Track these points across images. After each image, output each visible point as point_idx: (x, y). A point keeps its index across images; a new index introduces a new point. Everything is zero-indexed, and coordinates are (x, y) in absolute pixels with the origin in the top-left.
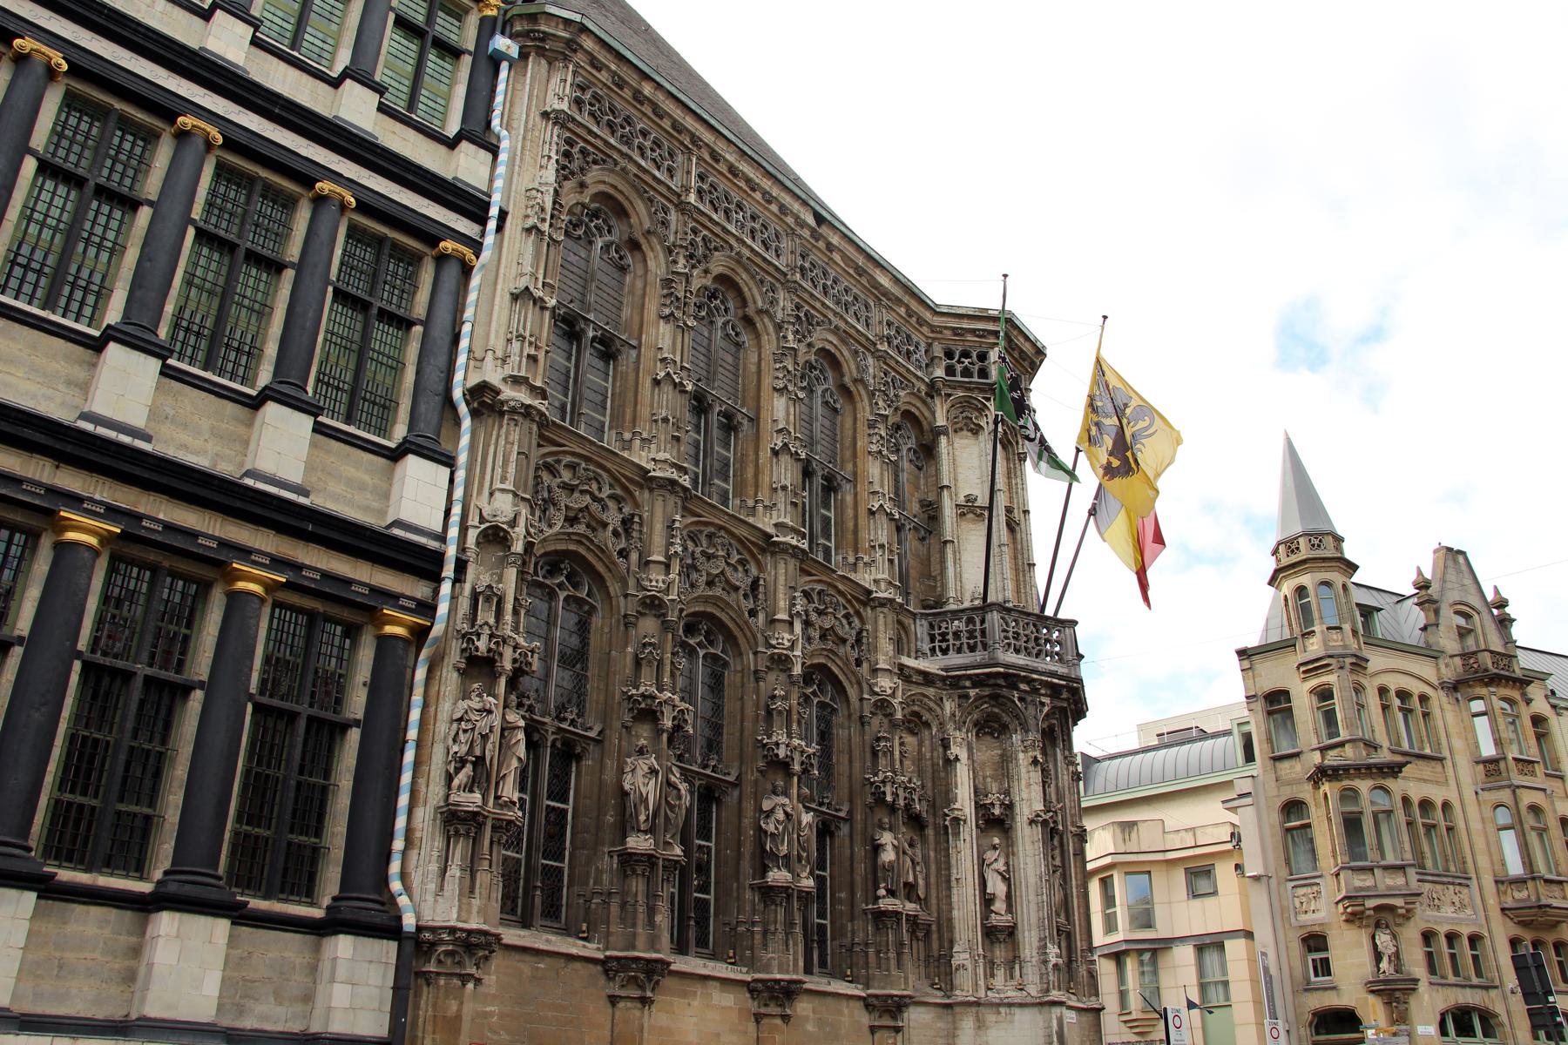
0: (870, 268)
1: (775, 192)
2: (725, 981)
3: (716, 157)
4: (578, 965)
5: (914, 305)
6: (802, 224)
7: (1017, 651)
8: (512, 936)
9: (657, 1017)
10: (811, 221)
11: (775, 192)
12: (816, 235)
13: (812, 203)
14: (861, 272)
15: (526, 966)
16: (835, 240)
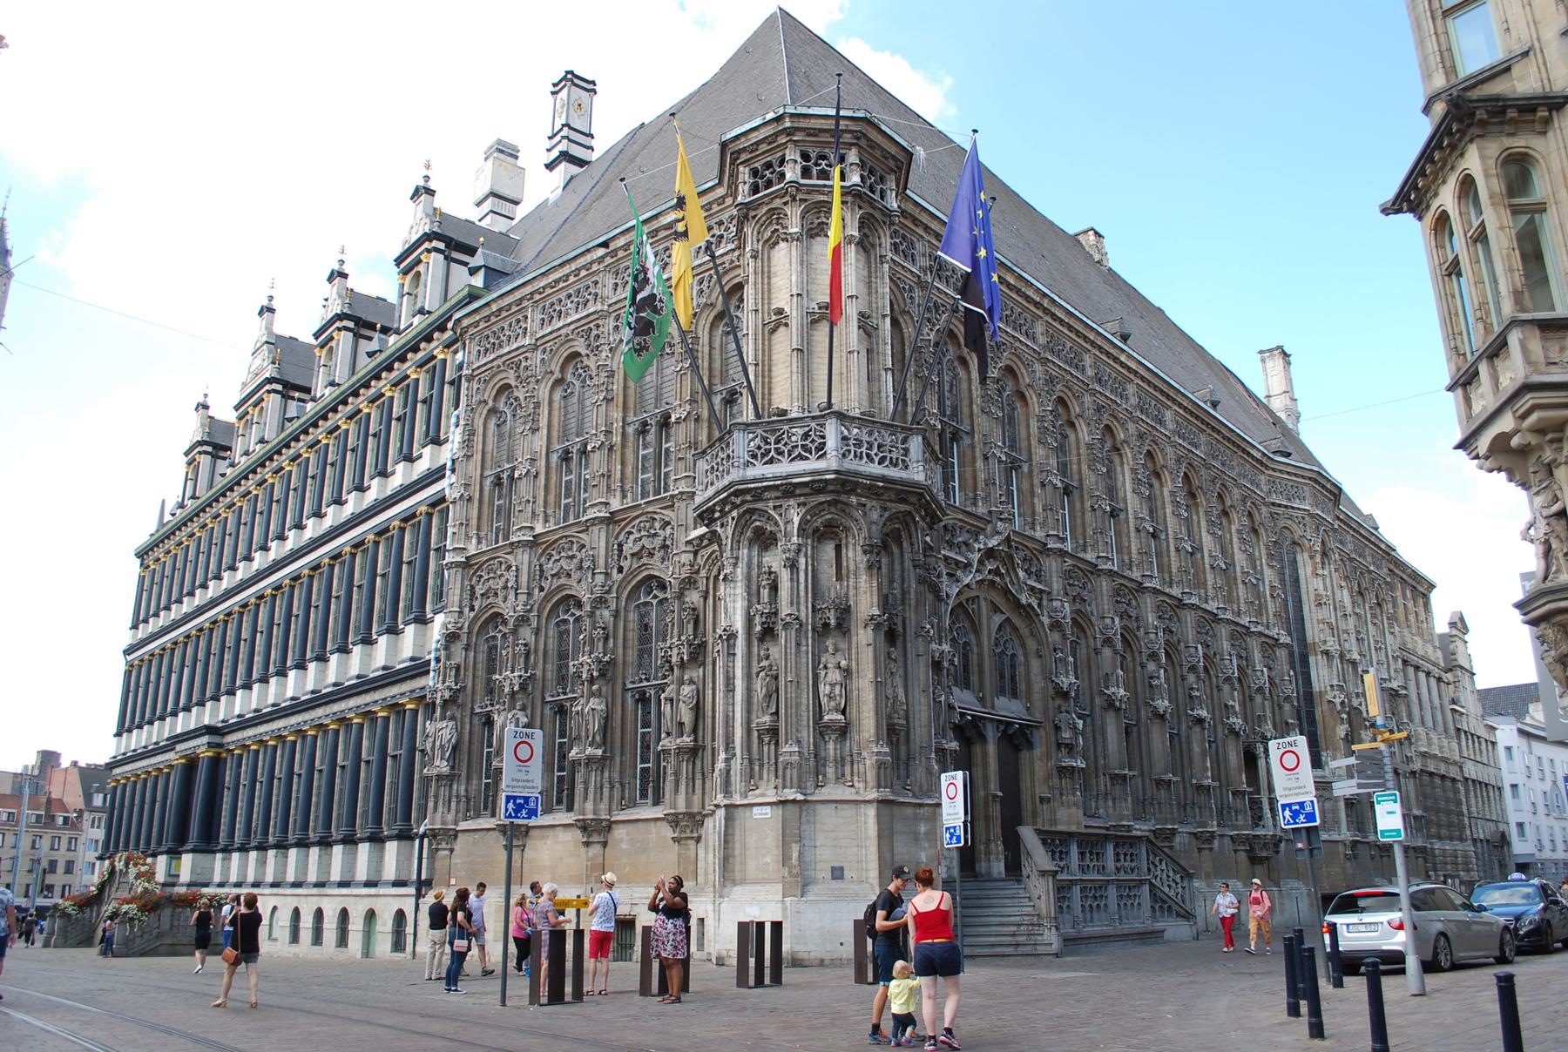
0: (655, 225)
1: (573, 266)
3: (537, 292)
6: (601, 260)
8: (463, 825)
9: (528, 853)
10: (601, 252)
11: (573, 266)
16: (622, 242)
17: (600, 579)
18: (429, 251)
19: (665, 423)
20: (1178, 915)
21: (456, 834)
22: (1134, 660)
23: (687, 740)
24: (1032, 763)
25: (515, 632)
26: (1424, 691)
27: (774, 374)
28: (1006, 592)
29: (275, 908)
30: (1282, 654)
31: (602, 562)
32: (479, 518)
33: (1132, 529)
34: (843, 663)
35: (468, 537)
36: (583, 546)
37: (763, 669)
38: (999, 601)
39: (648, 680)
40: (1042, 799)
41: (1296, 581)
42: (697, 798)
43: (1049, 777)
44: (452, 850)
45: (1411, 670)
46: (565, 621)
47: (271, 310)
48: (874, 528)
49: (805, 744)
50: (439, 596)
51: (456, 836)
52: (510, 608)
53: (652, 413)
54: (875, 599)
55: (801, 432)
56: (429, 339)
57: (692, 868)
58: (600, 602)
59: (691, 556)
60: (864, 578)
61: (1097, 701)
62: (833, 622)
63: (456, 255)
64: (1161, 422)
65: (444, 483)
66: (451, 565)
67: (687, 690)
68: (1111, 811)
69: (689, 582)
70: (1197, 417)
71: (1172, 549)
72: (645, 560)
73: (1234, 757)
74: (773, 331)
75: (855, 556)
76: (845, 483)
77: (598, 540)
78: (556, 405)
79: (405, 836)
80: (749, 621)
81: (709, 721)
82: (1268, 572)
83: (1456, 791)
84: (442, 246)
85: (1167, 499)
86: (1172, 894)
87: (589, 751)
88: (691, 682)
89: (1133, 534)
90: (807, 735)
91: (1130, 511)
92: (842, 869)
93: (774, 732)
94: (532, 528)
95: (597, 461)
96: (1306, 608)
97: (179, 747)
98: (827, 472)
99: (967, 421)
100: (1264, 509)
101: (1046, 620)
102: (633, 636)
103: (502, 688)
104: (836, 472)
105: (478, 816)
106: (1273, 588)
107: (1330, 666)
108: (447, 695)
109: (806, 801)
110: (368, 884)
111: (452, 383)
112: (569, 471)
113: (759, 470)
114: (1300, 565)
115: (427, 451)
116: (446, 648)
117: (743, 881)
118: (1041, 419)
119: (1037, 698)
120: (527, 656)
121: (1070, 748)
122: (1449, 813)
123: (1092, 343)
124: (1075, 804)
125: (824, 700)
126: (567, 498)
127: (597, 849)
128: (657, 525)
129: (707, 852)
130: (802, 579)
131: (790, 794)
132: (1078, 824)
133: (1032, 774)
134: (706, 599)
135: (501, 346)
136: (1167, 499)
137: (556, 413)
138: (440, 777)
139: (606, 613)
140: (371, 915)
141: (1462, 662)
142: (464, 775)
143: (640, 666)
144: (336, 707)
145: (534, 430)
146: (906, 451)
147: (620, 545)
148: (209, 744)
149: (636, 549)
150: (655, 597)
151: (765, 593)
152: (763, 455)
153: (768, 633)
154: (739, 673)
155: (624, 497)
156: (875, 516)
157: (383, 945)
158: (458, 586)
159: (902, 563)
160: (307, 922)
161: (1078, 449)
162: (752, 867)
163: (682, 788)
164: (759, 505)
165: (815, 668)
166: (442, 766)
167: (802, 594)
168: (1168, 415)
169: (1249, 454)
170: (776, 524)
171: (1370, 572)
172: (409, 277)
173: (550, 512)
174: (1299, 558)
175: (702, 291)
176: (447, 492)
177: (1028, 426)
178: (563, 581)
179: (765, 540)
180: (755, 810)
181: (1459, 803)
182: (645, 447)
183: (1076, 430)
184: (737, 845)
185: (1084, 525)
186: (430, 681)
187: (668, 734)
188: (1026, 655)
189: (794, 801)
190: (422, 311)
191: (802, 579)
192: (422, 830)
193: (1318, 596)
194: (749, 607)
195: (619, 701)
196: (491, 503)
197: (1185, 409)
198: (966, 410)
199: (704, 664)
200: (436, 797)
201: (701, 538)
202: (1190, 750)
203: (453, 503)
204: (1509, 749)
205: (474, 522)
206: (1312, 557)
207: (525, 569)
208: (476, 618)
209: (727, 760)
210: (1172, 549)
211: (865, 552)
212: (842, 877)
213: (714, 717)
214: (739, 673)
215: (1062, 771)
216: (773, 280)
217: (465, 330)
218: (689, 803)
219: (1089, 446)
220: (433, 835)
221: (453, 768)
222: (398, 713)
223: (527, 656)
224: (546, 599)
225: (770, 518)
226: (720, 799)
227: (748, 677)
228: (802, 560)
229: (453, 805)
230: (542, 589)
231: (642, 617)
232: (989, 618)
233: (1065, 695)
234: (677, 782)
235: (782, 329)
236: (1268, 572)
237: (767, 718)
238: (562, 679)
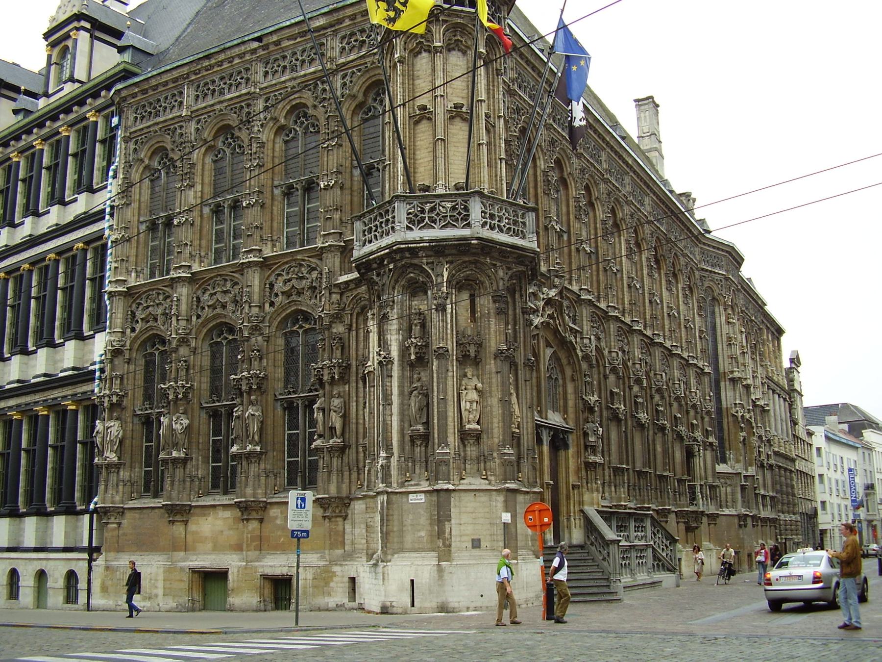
2: (225, 506)
4: (156, 510)
5: (349, 12)
6: (254, 51)
7: (370, 242)
9: (192, 527)
10: (256, 45)
12: (265, 47)
13: (246, 39)
14: (303, 34)
15: (137, 515)
16: (275, 38)
17: (255, 311)
18: (78, 29)
19: (310, 187)
20: (669, 570)
21: (122, 512)
22: (624, 384)
23: (336, 441)
24: (567, 460)
25: (176, 350)
26: (777, 407)
27: (418, 157)
28: (556, 332)
30: (706, 379)
31: (256, 297)
32: (137, 256)
33: (625, 285)
34: (479, 385)
35: (128, 272)
36: (236, 284)
37: (416, 388)
38: (550, 338)
39: (295, 393)
40: (574, 487)
41: (714, 328)
42: (345, 487)
43: (578, 470)
44: (119, 524)
45: (771, 392)
46: (218, 343)
48: (501, 284)
49: (452, 446)
51: (123, 513)
52: (173, 331)
53: (298, 179)
54: (503, 338)
55: (449, 205)
56: (81, 103)
57: (340, 539)
58: (256, 329)
59: (338, 297)
60: (493, 321)
61: (605, 413)
62: (473, 355)
63: (98, 34)
64: (642, 205)
65: (105, 224)
66: (111, 295)
67: (336, 402)
68: (613, 494)
69: (337, 317)
70: (664, 203)
71: (647, 301)
72: (294, 297)
73: (678, 455)
74: (417, 123)
75: (485, 303)
76: (487, 247)
77: (255, 280)
78: (207, 167)
80: (404, 351)
81: (354, 426)
82: (697, 319)
83: (792, 479)
84: (88, 26)
85: (645, 264)
86: (664, 554)
87: (249, 447)
88: (339, 396)
89: (626, 289)
90: (453, 439)
91: (624, 272)
92: (479, 540)
93: (426, 438)
94: (190, 267)
95: (252, 217)
96: (720, 347)
98: (472, 238)
99: (532, 199)
100: (697, 273)
101: (580, 354)
102: (281, 357)
103: (166, 396)
104: (478, 239)
106: (701, 331)
107: (734, 390)
108: (115, 399)
109: (454, 490)
110: (36, 550)
111: (103, 142)
112: (220, 222)
113: (416, 234)
114: (717, 315)
115: (83, 198)
116: (112, 361)
117: (402, 550)
118: (577, 200)
119: (571, 410)
120: (187, 370)
121: (594, 450)
122: (788, 494)
123: (608, 144)
124: (598, 491)
125: (465, 414)
126: (224, 245)
127: (254, 525)
128: (304, 270)
129: (353, 527)
130: (449, 321)
131: (442, 485)
132: (598, 504)
133: (567, 468)
134: (350, 330)
135: (157, 115)
136: (645, 264)
137: (207, 173)
138: (109, 466)
139: (260, 338)
140: (41, 575)
141: (797, 387)
143: (287, 381)
145: (192, 186)
146: (524, 223)
147: (272, 286)
149: (286, 288)
150: (301, 327)
151: (416, 330)
152: (419, 222)
153: (422, 361)
154: (395, 391)
155: (274, 246)
156: (501, 273)
157: (56, 597)
158: (121, 310)
159: (515, 309)
161: (595, 223)
162: (409, 539)
163: (334, 478)
164: (416, 261)
165: (459, 389)
167: (449, 331)
168: (647, 200)
169: (691, 231)
170: (429, 276)
171: (752, 321)
172: (56, 50)
173: (203, 254)
174: (717, 310)
175: (345, 84)
176: (107, 232)
177: (568, 206)
178: (219, 311)
179: (417, 289)
180: (411, 496)
181: (792, 487)
182: (289, 205)
183: (594, 210)
184: (396, 523)
185: (598, 281)
186: (96, 387)
187: (320, 436)
188: (564, 379)
189: (447, 490)
190: (72, 80)
191: (449, 321)
193: (729, 338)
194: (404, 340)
195: (270, 408)
196: (146, 244)
197: (658, 196)
198: (532, 191)
199: (348, 382)
200: (107, 481)
201: (346, 283)
202: (655, 450)
203: (114, 242)
204: (818, 449)
205: (132, 259)
206: (725, 310)
207: (184, 299)
208: (136, 338)
209: (388, 458)
210: (647, 301)
211: (494, 302)
212: (479, 546)
213: (357, 423)
214: (395, 391)
215: (589, 466)
216: (417, 82)
217: (124, 99)
218: (339, 489)
219: (604, 222)
221: (119, 458)
222: (57, 413)
223: (187, 370)
224: (203, 325)
225: (424, 271)
226: (381, 486)
227: (401, 393)
228: (449, 306)
229: (121, 488)
230: (198, 317)
231: (287, 343)
232: (544, 351)
233: (591, 410)
234: (330, 473)
235: (424, 121)
236: (697, 319)
237: (420, 427)
238: (215, 391)
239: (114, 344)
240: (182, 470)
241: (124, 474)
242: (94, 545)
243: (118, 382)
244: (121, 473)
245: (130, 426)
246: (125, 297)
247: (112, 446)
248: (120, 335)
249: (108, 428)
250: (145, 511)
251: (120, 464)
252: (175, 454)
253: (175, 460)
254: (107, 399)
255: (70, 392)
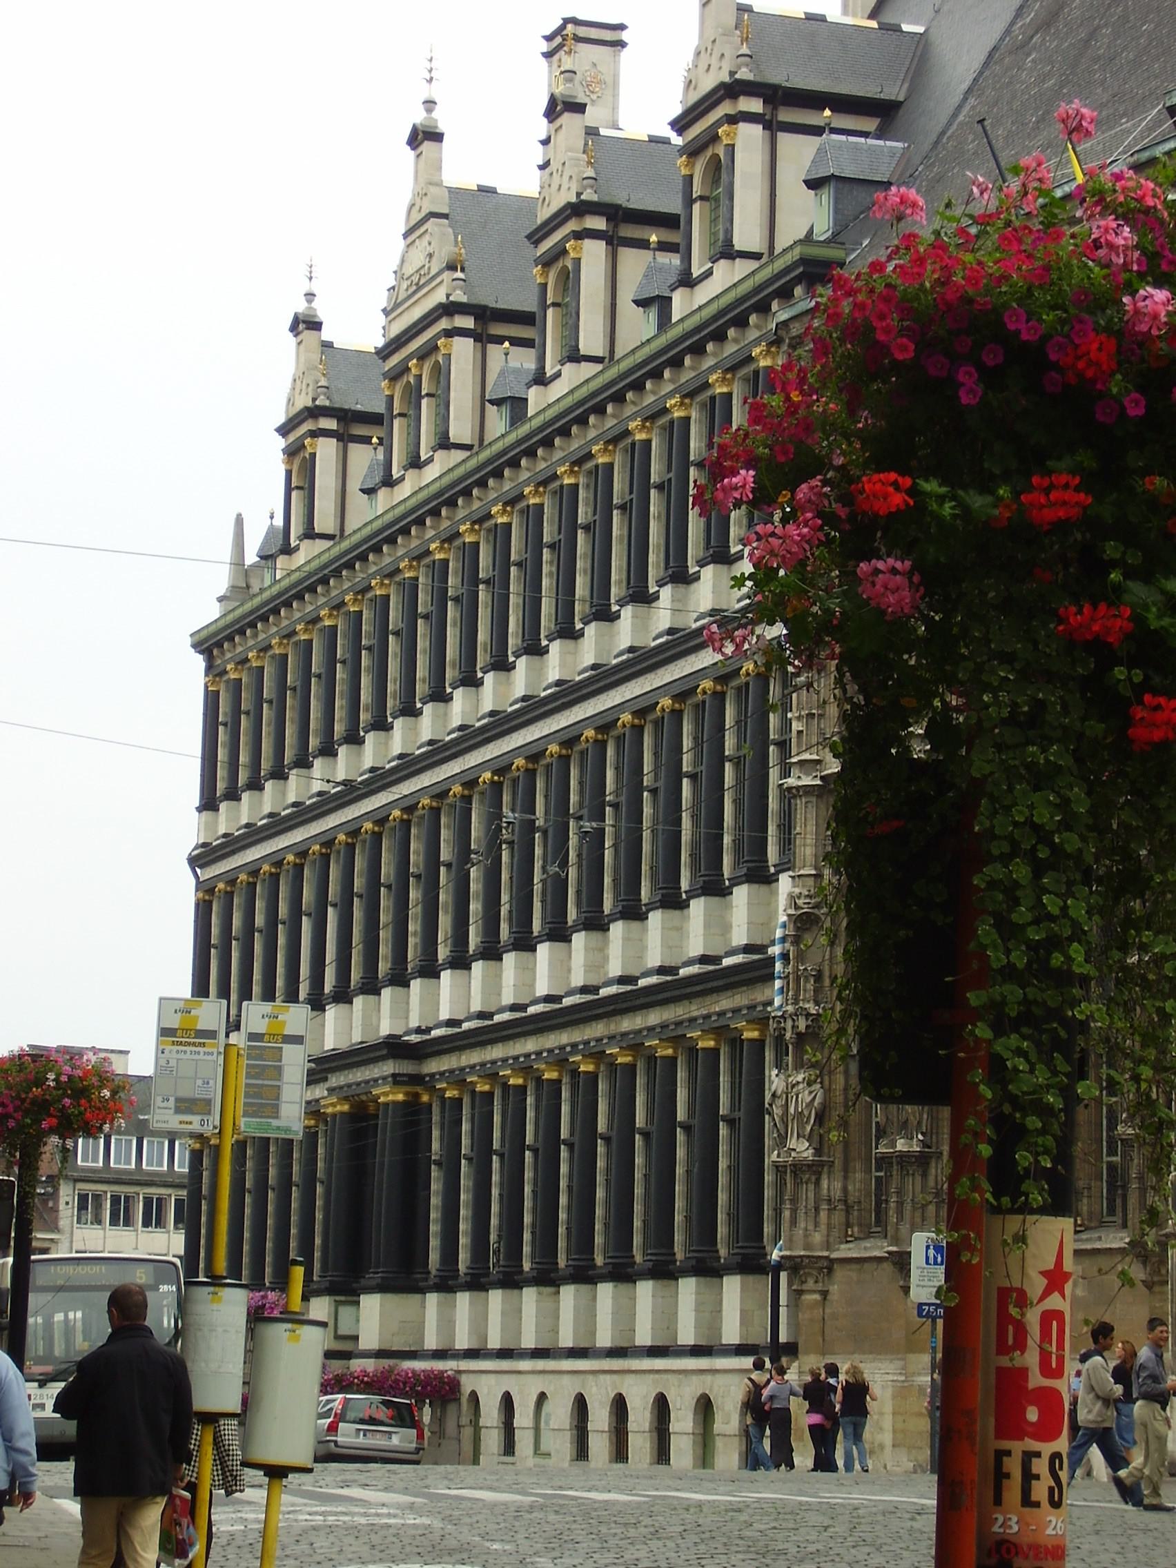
18: (732, 120)
21: (829, 1267)
29: (542, 1397)
44: (825, 1294)
47: (437, 137)
50: (787, 842)
51: (830, 1270)
79: (751, 1263)
97: (336, 1080)
105: (868, 1235)
108: (802, 1024)
110: (697, 1351)
138: (798, 1168)
142: (838, 1164)
144: (627, 1024)
148: (397, 1080)
160: (600, 1418)
166: (802, 1149)
192: (775, 1255)
220: (794, 1266)
221: (818, 1152)
229: (823, 1215)
239: (800, 902)
240: (918, 1179)
241: (831, 1185)
242: (783, 1338)
243: (810, 986)
244: (825, 1184)
245: (840, 1080)
246: (819, 796)
247: (801, 1126)
248: (811, 881)
249: (793, 1086)
250: (866, 1265)
251: (821, 1164)
252: (901, 1145)
253: (903, 1158)
254: (789, 1023)
255: (745, 1002)
